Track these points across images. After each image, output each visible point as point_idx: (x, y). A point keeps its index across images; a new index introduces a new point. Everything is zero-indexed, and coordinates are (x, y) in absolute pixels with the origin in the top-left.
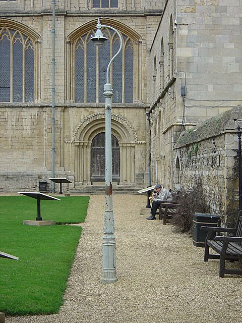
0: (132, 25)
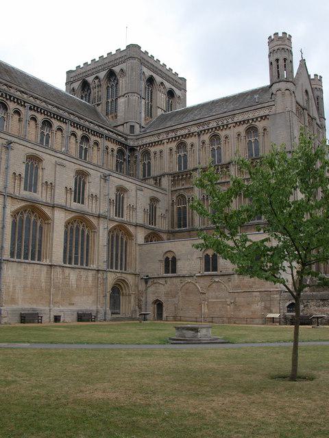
0: (131, 229)
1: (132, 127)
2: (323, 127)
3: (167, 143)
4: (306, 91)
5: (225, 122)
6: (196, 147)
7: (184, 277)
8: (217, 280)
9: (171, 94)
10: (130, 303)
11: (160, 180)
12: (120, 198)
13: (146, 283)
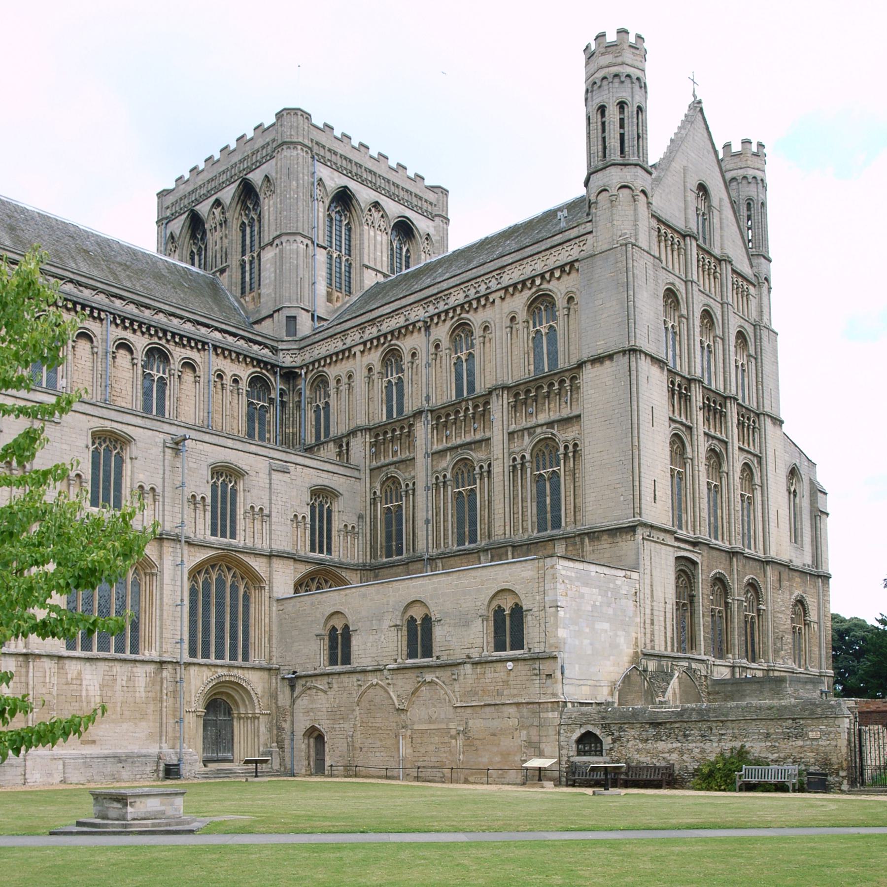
1: (292, 319)
2: (762, 282)
3: (362, 352)
4: (702, 188)
5: (483, 289)
6: (422, 358)
7: (364, 672)
8: (429, 677)
9: (404, 229)
10: (256, 733)
11: (348, 444)
12: (224, 492)
13: (292, 688)
